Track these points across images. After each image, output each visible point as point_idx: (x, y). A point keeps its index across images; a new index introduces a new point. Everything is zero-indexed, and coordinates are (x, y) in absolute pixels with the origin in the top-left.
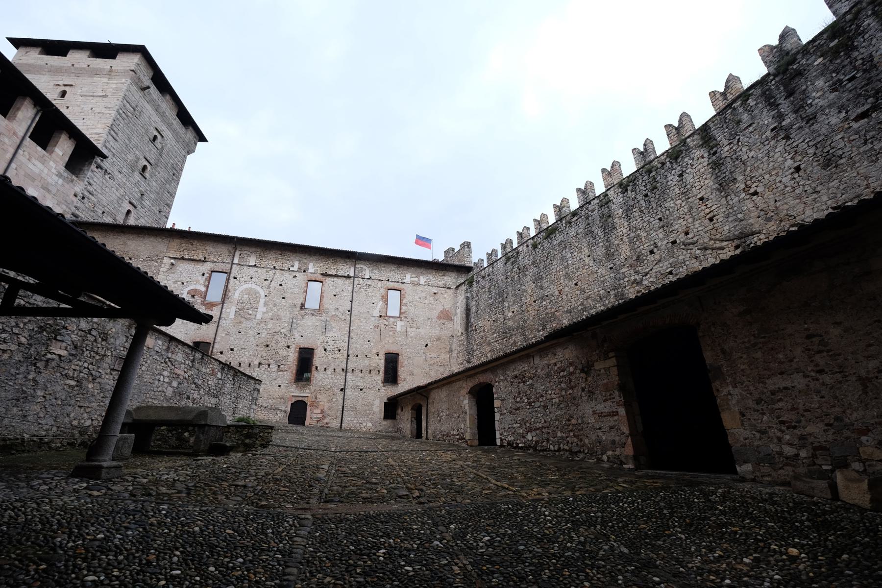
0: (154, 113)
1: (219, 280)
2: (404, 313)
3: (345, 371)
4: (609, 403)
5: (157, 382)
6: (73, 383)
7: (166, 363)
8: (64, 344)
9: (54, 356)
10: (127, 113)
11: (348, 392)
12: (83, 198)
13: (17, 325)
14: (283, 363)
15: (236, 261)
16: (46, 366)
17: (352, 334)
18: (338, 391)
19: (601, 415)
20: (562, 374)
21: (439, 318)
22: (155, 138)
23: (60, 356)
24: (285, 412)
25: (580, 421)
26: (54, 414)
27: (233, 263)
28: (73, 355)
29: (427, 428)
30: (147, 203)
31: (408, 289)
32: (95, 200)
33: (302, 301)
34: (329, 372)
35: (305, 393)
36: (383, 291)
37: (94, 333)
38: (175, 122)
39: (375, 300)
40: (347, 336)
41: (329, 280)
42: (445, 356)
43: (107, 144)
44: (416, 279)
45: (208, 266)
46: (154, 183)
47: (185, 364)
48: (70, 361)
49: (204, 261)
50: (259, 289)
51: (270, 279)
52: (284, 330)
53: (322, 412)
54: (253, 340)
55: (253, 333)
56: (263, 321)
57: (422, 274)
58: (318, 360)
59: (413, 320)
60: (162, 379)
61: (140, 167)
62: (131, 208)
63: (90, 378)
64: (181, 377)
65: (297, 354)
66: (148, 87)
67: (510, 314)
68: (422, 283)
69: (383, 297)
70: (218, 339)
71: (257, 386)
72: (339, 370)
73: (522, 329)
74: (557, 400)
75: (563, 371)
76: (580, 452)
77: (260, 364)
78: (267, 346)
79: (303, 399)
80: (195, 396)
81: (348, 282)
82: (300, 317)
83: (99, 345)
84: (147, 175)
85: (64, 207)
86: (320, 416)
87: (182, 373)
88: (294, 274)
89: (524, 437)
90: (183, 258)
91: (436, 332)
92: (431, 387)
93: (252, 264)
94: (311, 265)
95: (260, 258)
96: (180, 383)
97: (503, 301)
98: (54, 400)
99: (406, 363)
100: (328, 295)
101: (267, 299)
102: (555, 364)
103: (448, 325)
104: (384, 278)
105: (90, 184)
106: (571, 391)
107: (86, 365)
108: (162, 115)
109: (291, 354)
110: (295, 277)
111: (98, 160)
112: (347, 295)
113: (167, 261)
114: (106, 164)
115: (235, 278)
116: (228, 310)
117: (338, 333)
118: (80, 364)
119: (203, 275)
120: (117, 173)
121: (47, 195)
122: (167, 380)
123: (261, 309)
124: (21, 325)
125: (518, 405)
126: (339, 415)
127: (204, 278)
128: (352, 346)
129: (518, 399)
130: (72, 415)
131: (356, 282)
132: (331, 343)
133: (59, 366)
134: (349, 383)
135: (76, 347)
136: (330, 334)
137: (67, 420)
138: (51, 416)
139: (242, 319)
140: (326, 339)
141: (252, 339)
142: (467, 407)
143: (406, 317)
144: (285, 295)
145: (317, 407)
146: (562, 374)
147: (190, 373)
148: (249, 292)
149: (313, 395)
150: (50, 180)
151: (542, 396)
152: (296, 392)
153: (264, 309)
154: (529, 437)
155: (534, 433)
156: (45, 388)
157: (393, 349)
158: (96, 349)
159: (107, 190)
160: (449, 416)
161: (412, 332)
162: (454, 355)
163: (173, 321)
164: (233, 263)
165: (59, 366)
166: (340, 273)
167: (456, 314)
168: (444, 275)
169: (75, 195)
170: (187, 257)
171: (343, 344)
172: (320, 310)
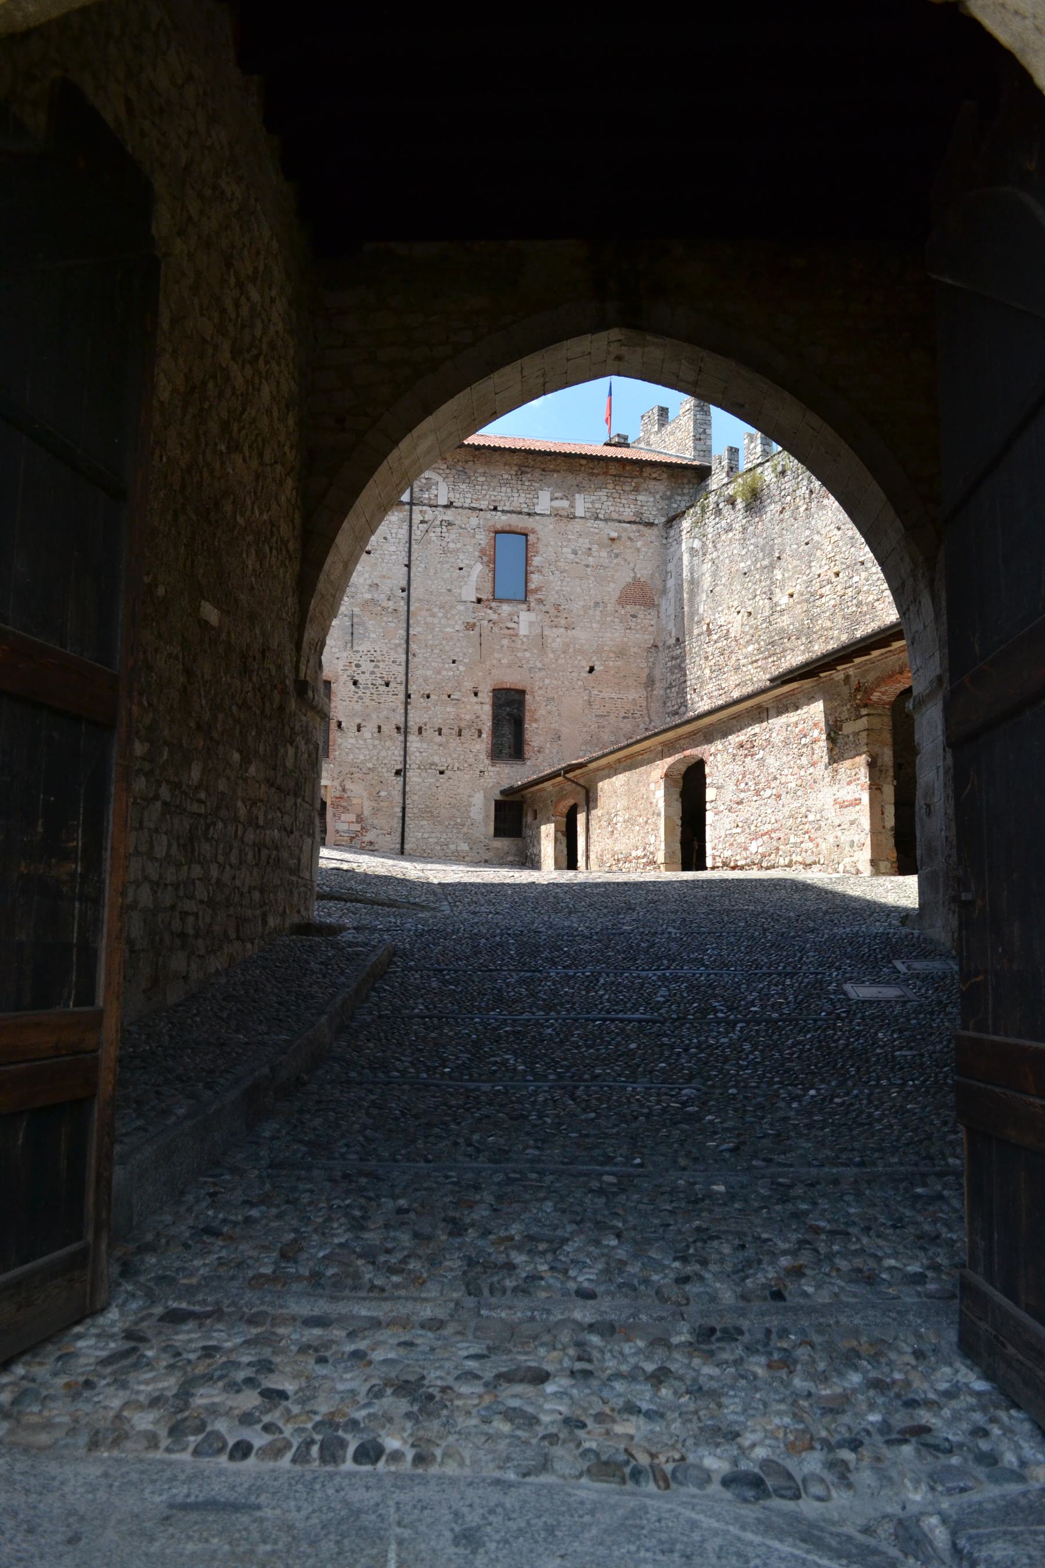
2: (537, 590)
3: (403, 730)
4: (853, 786)
11: (413, 776)
17: (413, 646)
18: (390, 776)
19: (843, 805)
20: (803, 741)
21: (624, 600)
25: (818, 817)
29: (587, 850)
31: (544, 530)
34: (366, 733)
36: (483, 538)
39: (463, 560)
40: (401, 651)
42: (635, 694)
44: (565, 503)
53: (360, 819)
57: (580, 488)
59: (557, 607)
67: (784, 601)
68: (580, 512)
69: (483, 552)
72: (388, 729)
73: (806, 633)
74: (793, 785)
75: (805, 736)
76: (815, 863)
86: (357, 827)
89: (746, 849)
91: (615, 635)
92: (593, 766)
97: (772, 567)
99: (542, 711)
102: (796, 724)
103: (646, 618)
104: (483, 504)
106: (811, 770)
125: (742, 795)
126: (396, 824)
128: (416, 674)
129: (742, 786)
131: (417, 517)
132: (367, 666)
134: (414, 758)
136: (363, 647)
142: (661, 804)
143: (540, 601)
145: (346, 810)
146: (803, 741)
149: (336, 783)
151: (775, 778)
154: (753, 848)
155: (760, 841)
157: (511, 679)
160: (630, 821)
161: (556, 637)
162: (658, 691)
167: (664, 591)
168: (636, 490)
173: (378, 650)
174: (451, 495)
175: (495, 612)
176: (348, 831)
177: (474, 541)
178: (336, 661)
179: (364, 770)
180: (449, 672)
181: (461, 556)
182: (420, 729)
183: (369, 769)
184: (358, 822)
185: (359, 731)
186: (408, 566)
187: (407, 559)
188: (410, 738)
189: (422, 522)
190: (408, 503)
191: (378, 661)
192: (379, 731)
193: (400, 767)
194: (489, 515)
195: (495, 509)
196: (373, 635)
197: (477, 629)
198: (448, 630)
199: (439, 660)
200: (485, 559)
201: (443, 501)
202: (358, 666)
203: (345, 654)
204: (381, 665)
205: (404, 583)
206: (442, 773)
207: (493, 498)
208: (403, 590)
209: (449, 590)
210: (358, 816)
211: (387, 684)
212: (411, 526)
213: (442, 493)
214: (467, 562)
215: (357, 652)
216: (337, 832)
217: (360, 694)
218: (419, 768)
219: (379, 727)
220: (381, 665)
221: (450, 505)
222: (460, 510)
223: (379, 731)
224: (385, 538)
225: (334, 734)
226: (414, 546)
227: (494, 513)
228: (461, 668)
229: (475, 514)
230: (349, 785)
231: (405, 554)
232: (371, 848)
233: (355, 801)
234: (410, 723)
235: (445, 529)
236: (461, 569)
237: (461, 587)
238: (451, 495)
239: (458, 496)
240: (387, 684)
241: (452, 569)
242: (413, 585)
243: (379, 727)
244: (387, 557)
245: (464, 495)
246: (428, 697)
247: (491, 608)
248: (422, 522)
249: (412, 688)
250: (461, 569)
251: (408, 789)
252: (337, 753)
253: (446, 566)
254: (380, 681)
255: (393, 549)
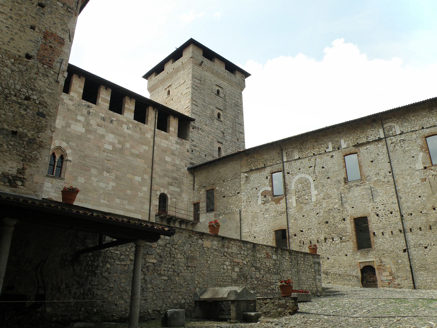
0: (214, 75)
1: (278, 177)
3: (403, 231)
5: (222, 270)
6: (166, 278)
7: (226, 256)
8: (154, 256)
9: (150, 264)
10: (198, 86)
11: (413, 251)
12: (192, 151)
13: (126, 250)
14: (344, 235)
15: (285, 160)
16: (148, 270)
17: (400, 194)
18: (402, 253)
22: (218, 91)
23: (154, 263)
24: (357, 277)
26: (162, 297)
27: (283, 162)
28: (160, 261)
30: (228, 137)
32: (199, 149)
33: (344, 175)
35: (370, 258)
36: (420, 141)
37: (168, 246)
38: (226, 74)
39: (414, 153)
40: (395, 197)
41: (362, 150)
43: (194, 111)
45: (268, 170)
46: (228, 122)
47: (240, 254)
48: (160, 265)
49: (265, 167)
50: (308, 177)
51: (313, 165)
52: (336, 206)
53: (391, 274)
54: (315, 221)
55: (313, 214)
56: (318, 203)
58: (374, 225)
60: (225, 267)
61: (216, 116)
62: (220, 145)
63: (176, 274)
64: (240, 264)
65: (353, 225)
66: (202, 62)
69: (422, 147)
70: (290, 225)
71: (316, 260)
77: (325, 239)
78: (327, 222)
79: (370, 264)
80: (258, 275)
81: (380, 145)
82: (346, 191)
83: (174, 253)
84: (222, 119)
85: (185, 161)
86: (391, 278)
87: (241, 261)
88: (331, 154)
90: (251, 170)
93: (297, 157)
94: (342, 141)
95: (301, 150)
96: (241, 269)
98: (158, 289)
100: (366, 163)
101: (316, 183)
104: (417, 128)
105: (193, 141)
107: (170, 266)
108: (216, 74)
109: (348, 226)
110: (332, 156)
111: (192, 123)
112: (383, 158)
113: (243, 175)
114: (196, 124)
115: (288, 173)
116: (290, 201)
117: (385, 197)
118: (166, 266)
119: (267, 178)
120: (204, 126)
121: (175, 157)
122: (229, 267)
123: (314, 192)
124: (128, 250)
127: (268, 180)
128: (404, 206)
130: (172, 297)
131: (389, 142)
133: (154, 269)
134: (411, 243)
135: (161, 257)
136: (377, 200)
137: (170, 300)
138: (160, 299)
139: (302, 205)
140: (376, 205)
141: (314, 219)
144: (329, 175)
147: (247, 260)
148: (301, 181)
149: (378, 259)
150: (173, 148)
152: (362, 258)
153: (316, 192)
156: (151, 283)
158: (173, 256)
159: (203, 140)
163: (159, 238)
164: (283, 162)
165: (154, 269)
166: (371, 139)
169: (188, 152)
170: (253, 168)
171: (393, 205)
172: (363, 179)
173: (384, 199)
174: (402, 129)
175: (434, 171)
176: (387, 280)
177: (417, 144)
178: (367, 208)
179: (389, 252)
180: (418, 201)
181: (412, 152)
182: (411, 229)
183: (391, 251)
184: (390, 275)
185: (383, 235)
186: (390, 162)
187: (388, 160)
188: (407, 234)
189: (391, 143)
190: (384, 138)
191: (385, 204)
192: (392, 234)
193: (405, 248)
194: (420, 132)
195: (423, 128)
196: (381, 194)
197: (427, 180)
198: (414, 184)
199: (413, 198)
200: (423, 150)
201: (398, 132)
202: (377, 208)
203: (371, 204)
204: (387, 205)
205: (389, 170)
206: (426, 248)
207: (420, 124)
208: (390, 172)
209: (410, 167)
210: (390, 273)
211: (391, 213)
212: (387, 147)
213: (397, 129)
214: (416, 153)
215: (376, 202)
216: (382, 281)
217: (380, 219)
218: (414, 247)
219: (392, 232)
220: (387, 205)
221: (402, 133)
222: (407, 134)
223: (392, 234)
224: (378, 154)
225: (372, 238)
226: (391, 154)
227: (423, 130)
228: (424, 199)
229: (414, 133)
230: (383, 259)
231: (387, 158)
232: (399, 287)
233: (387, 266)
234: (406, 228)
235: (402, 143)
236: (413, 157)
237: (415, 165)
238: (402, 129)
239: (404, 128)
240: (391, 213)
241: (409, 158)
242: (394, 169)
243: (392, 232)
244: (380, 161)
245: (407, 127)
246: (411, 214)
247: (432, 170)
248: (391, 143)
249: (403, 212)
250: (413, 157)
251: (411, 258)
252: (375, 246)
253: (406, 158)
254: (388, 212)
255: (382, 157)
